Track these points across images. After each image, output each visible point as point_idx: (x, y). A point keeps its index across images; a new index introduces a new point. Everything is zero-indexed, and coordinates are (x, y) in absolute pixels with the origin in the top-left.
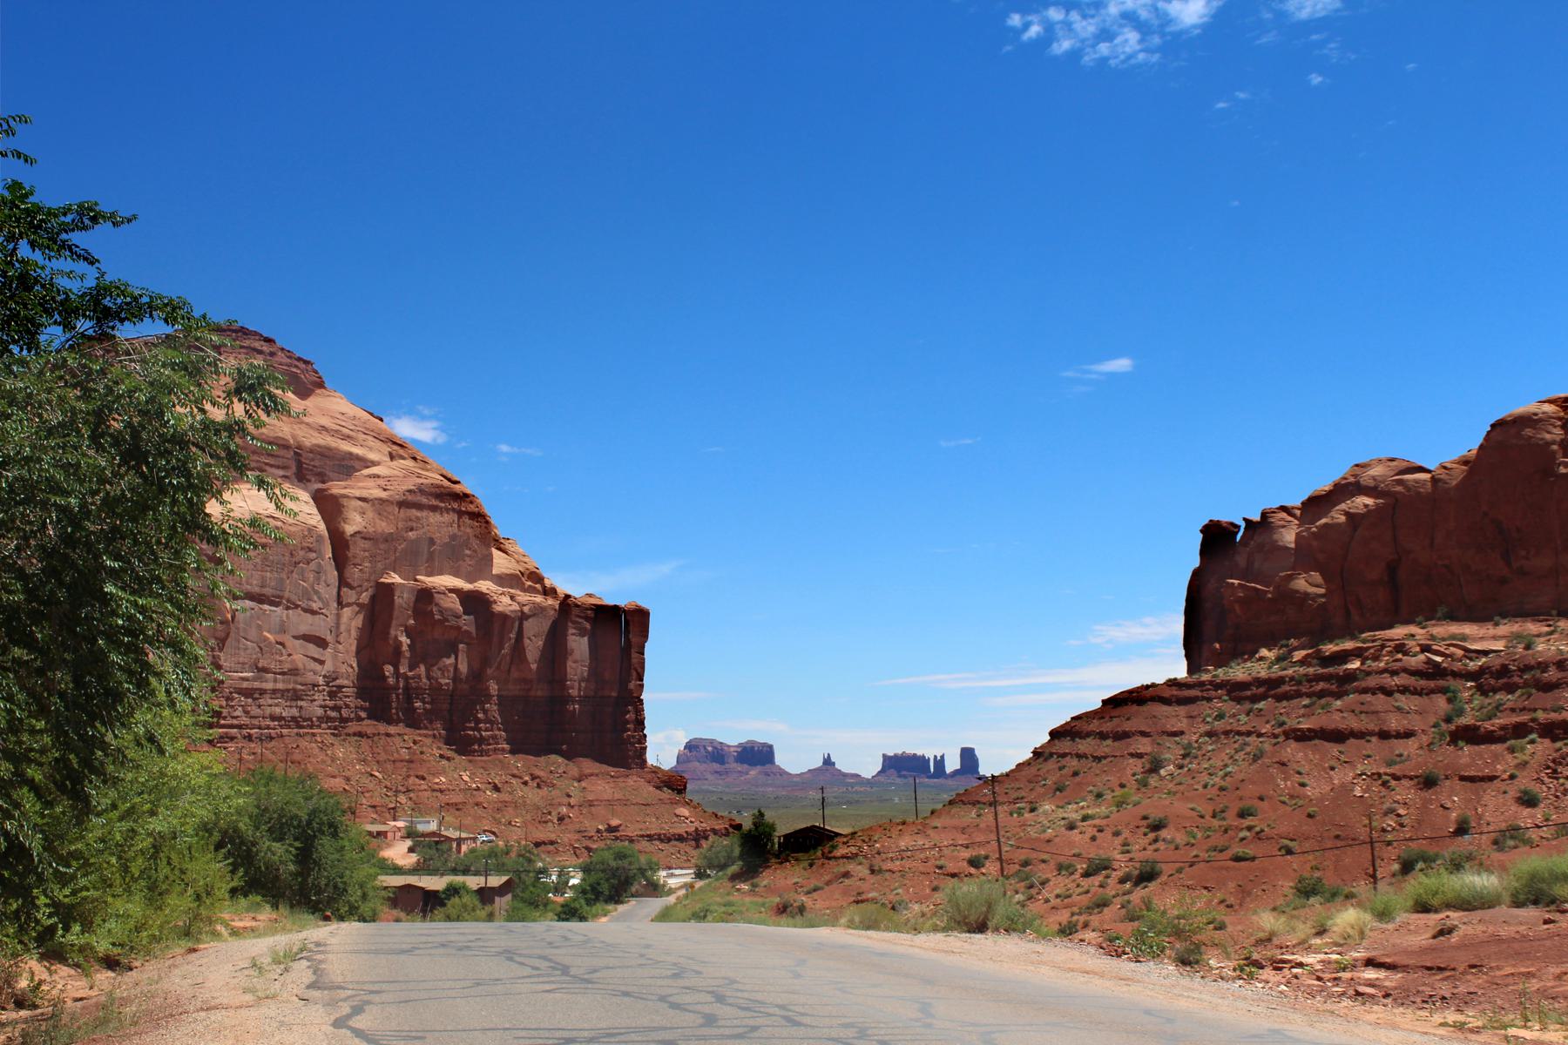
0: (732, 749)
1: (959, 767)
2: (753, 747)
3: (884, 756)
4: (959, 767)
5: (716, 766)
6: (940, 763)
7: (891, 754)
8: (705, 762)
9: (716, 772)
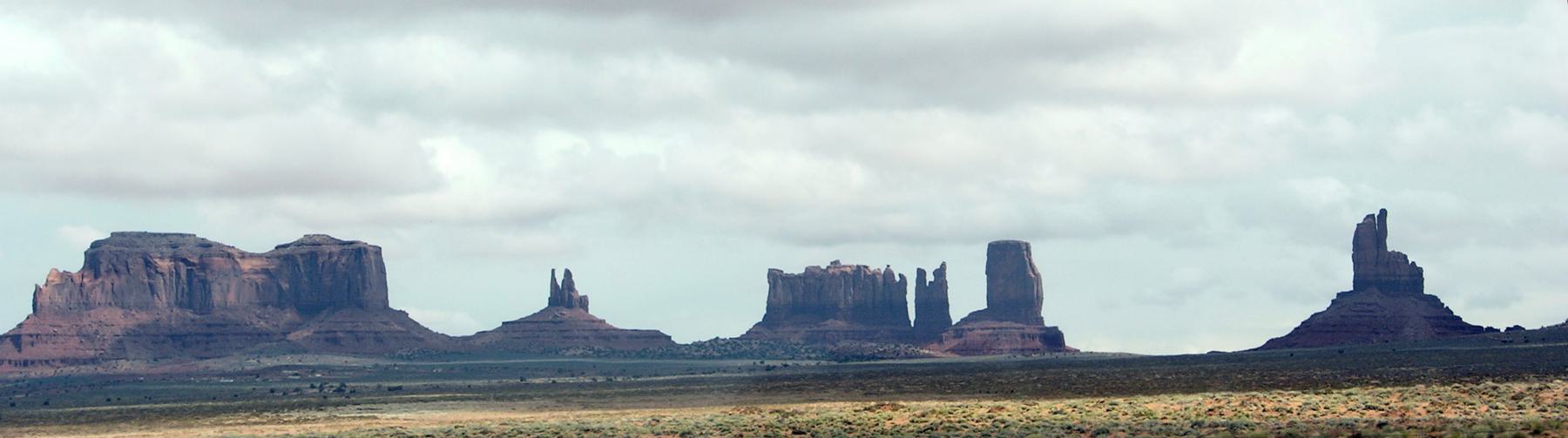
3: (775, 277)
6: (934, 291)
7: (795, 265)
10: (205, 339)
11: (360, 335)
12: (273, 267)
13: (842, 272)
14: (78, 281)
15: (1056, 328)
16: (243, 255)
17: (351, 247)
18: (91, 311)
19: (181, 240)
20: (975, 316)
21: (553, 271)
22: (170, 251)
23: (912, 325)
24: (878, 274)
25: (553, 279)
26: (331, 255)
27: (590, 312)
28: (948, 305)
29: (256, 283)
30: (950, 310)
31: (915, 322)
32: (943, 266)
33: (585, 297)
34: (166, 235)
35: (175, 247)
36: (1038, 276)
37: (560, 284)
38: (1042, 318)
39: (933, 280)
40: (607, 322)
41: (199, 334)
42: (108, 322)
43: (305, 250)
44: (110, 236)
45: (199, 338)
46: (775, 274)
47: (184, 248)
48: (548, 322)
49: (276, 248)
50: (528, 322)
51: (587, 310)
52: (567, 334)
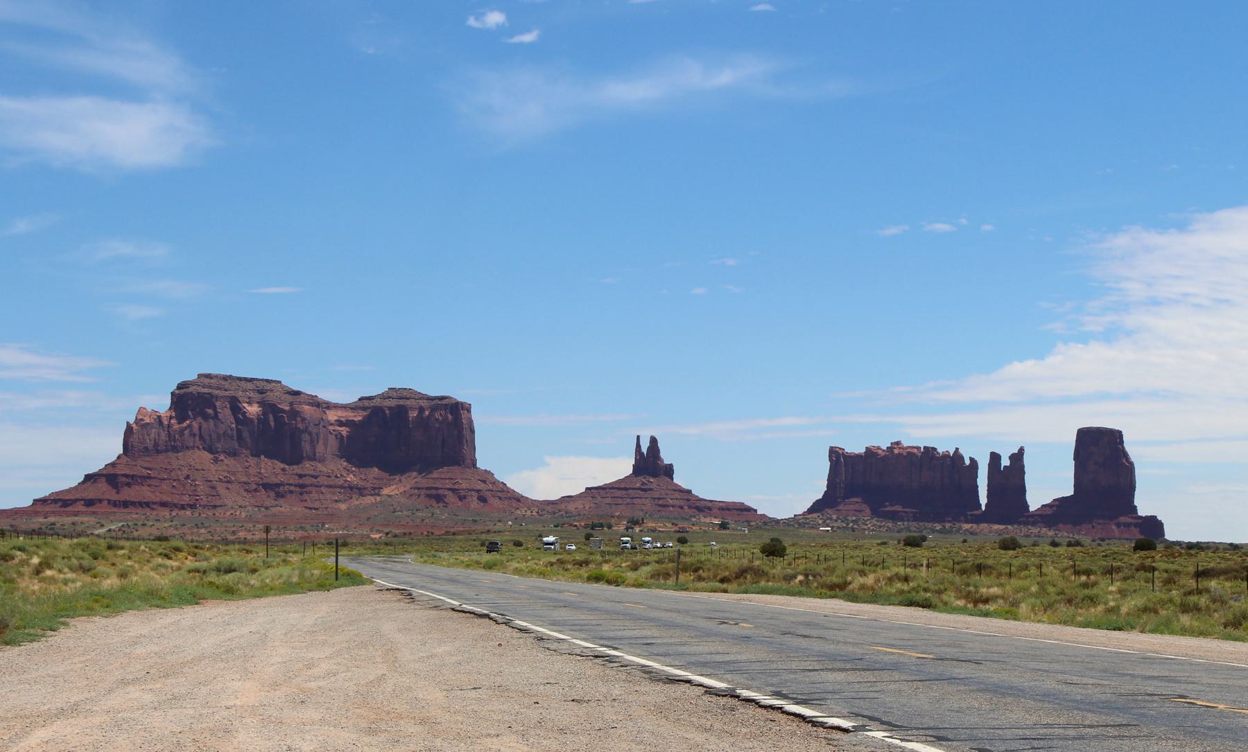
0: (332, 416)
1: (1069, 491)
2: (401, 411)
3: (836, 455)
4: (1069, 491)
5: (270, 469)
7: (856, 447)
8: (233, 454)
9: (267, 487)
10: (298, 489)
11: (463, 493)
12: (360, 418)
13: (909, 453)
14: (166, 423)
15: (1153, 518)
16: (329, 406)
17: (444, 402)
18: (180, 454)
19: (269, 386)
20: (1061, 502)
21: (638, 437)
22: (257, 396)
23: (983, 508)
24: (949, 456)
25: (638, 446)
26: (421, 410)
27: (675, 481)
28: (1025, 491)
29: (342, 436)
30: (1027, 496)
31: (987, 505)
32: (1021, 450)
33: (671, 466)
34: (251, 380)
35: (261, 392)
36: (1132, 464)
37: (644, 450)
38: (1136, 507)
39: (1008, 465)
40: (693, 492)
41: (291, 485)
42: (198, 466)
43: (393, 403)
44: (197, 377)
45: (292, 488)
46: (837, 452)
47: (271, 394)
48: (636, 489)
49: (360, 400)
50: (613, 488)
51: (672, 479)
52: (660, 502)
